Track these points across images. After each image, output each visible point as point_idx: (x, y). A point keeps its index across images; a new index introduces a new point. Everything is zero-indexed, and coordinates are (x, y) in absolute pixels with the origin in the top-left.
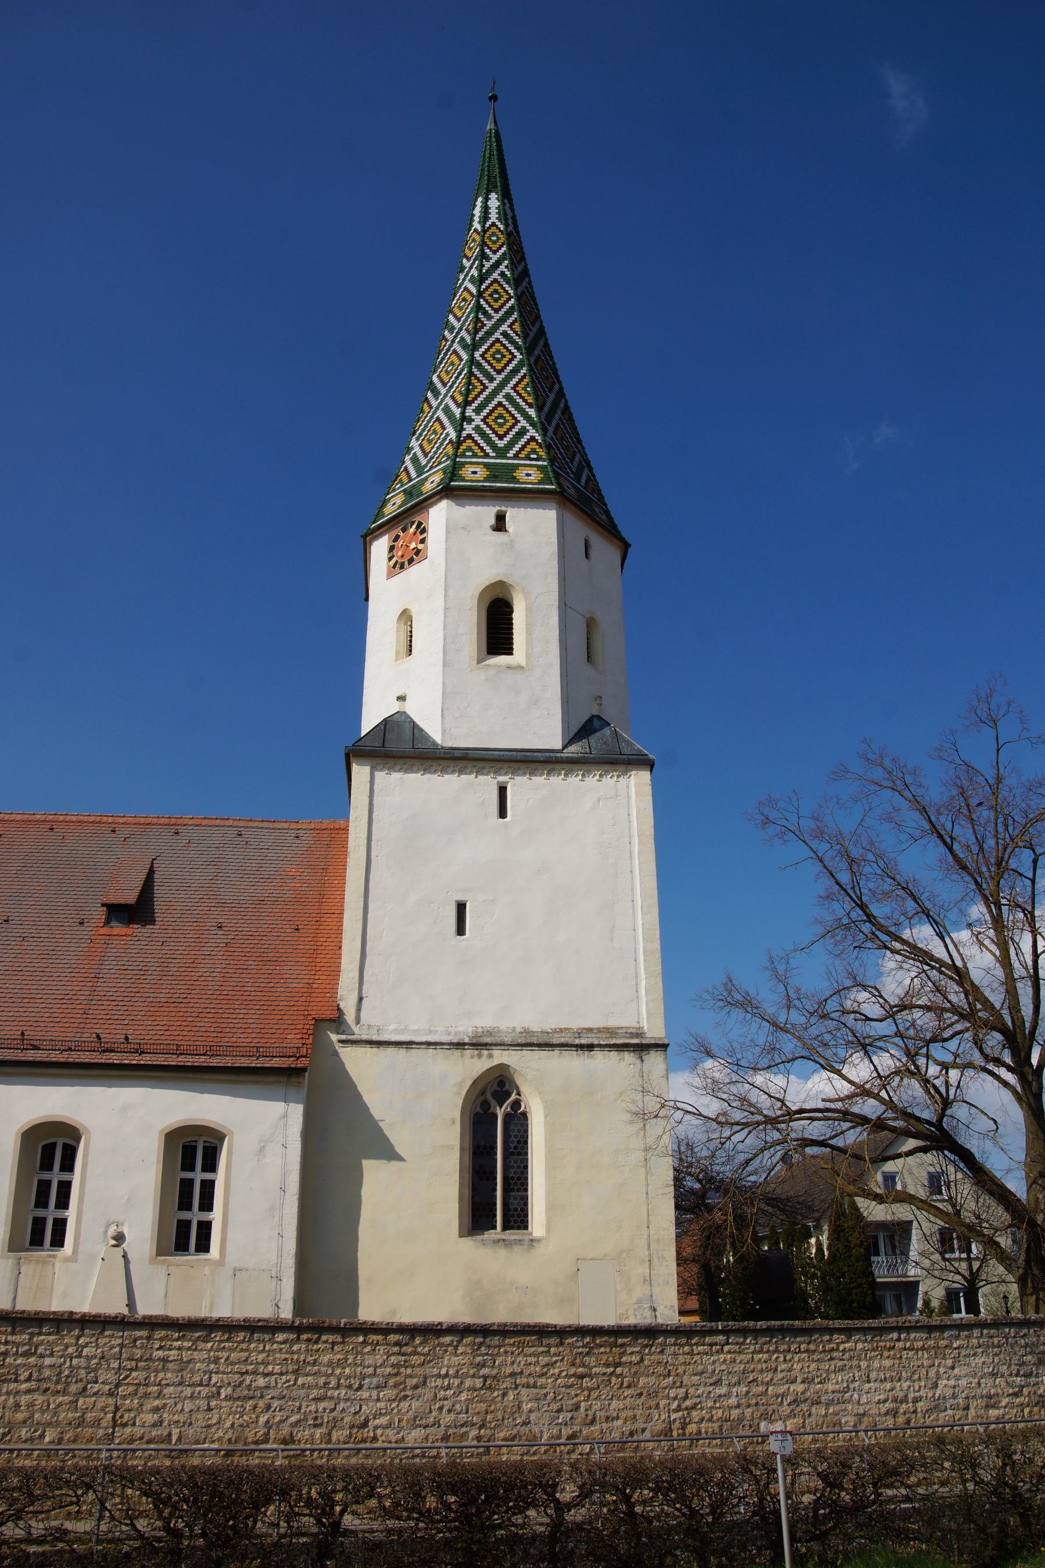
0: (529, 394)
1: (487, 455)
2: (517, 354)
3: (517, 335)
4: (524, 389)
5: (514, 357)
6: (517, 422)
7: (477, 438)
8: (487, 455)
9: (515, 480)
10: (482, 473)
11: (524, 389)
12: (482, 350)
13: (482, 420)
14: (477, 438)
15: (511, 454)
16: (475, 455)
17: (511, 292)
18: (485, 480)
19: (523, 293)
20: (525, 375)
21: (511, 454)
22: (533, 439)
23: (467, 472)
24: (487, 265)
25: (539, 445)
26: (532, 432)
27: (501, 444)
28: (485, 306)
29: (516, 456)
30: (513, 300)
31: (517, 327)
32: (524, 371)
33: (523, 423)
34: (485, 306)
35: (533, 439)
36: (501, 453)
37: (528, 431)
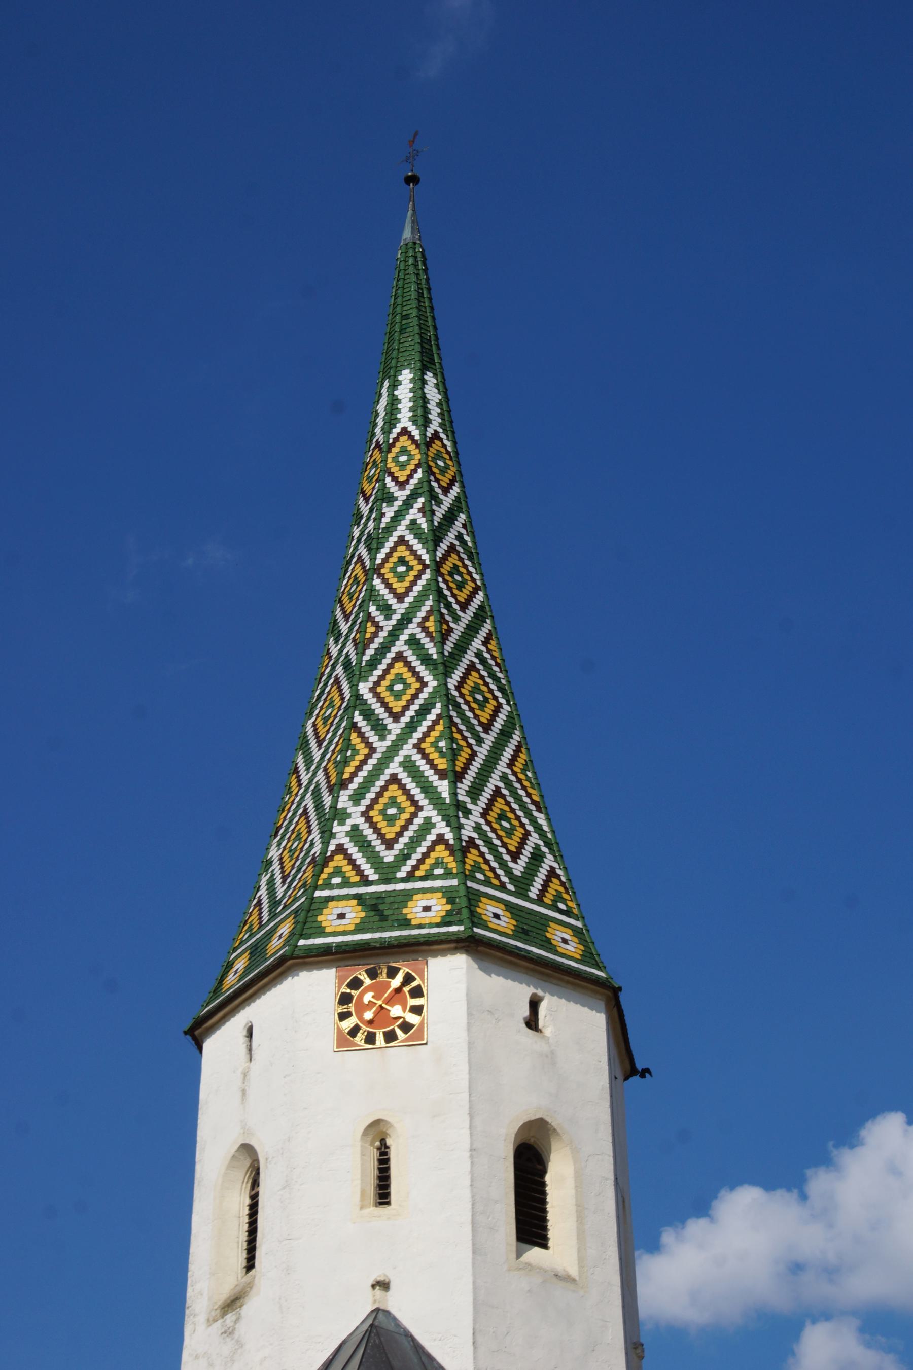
0: (442, 754)
1: (365, 882)
2: (428, 677)
3: (432, 639)
4: (434, 745)
5: (425, 684)
6: (420, 809)
7: (353, 850)
8: (365, 882)
9: (406, 923)
10: (354, 914)
11: (434, 745)
12: (373, 679)
13: (363, 814)
14: (353, 850)
15: (401, 874)
16: (346, 883)
17: (426, 557)
18: (358, 929)
19: (445, 557)
20: (439, 717)
21: (401, 874)
22: (440, 839)
23: (328, 918)
24: (389, 512)
25: (448, 846)
26: (441, 827)
27: (389, 857)
28: (384, 591)
29: (410, 877)
30: (428, 571)
31: (431, 624)
32: (437, 710)
33: (429, 811)
34: (384, 591)
35: (440, 839)
36: (387, 873)
37: (434, 825)
